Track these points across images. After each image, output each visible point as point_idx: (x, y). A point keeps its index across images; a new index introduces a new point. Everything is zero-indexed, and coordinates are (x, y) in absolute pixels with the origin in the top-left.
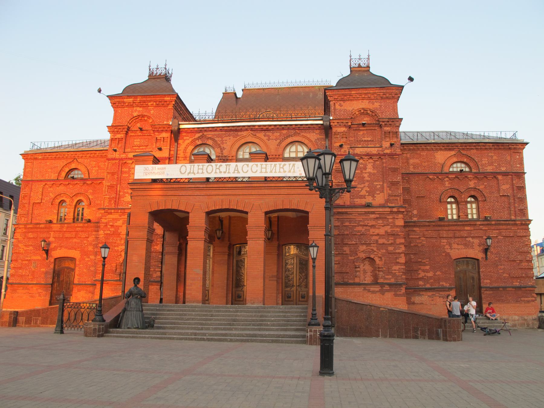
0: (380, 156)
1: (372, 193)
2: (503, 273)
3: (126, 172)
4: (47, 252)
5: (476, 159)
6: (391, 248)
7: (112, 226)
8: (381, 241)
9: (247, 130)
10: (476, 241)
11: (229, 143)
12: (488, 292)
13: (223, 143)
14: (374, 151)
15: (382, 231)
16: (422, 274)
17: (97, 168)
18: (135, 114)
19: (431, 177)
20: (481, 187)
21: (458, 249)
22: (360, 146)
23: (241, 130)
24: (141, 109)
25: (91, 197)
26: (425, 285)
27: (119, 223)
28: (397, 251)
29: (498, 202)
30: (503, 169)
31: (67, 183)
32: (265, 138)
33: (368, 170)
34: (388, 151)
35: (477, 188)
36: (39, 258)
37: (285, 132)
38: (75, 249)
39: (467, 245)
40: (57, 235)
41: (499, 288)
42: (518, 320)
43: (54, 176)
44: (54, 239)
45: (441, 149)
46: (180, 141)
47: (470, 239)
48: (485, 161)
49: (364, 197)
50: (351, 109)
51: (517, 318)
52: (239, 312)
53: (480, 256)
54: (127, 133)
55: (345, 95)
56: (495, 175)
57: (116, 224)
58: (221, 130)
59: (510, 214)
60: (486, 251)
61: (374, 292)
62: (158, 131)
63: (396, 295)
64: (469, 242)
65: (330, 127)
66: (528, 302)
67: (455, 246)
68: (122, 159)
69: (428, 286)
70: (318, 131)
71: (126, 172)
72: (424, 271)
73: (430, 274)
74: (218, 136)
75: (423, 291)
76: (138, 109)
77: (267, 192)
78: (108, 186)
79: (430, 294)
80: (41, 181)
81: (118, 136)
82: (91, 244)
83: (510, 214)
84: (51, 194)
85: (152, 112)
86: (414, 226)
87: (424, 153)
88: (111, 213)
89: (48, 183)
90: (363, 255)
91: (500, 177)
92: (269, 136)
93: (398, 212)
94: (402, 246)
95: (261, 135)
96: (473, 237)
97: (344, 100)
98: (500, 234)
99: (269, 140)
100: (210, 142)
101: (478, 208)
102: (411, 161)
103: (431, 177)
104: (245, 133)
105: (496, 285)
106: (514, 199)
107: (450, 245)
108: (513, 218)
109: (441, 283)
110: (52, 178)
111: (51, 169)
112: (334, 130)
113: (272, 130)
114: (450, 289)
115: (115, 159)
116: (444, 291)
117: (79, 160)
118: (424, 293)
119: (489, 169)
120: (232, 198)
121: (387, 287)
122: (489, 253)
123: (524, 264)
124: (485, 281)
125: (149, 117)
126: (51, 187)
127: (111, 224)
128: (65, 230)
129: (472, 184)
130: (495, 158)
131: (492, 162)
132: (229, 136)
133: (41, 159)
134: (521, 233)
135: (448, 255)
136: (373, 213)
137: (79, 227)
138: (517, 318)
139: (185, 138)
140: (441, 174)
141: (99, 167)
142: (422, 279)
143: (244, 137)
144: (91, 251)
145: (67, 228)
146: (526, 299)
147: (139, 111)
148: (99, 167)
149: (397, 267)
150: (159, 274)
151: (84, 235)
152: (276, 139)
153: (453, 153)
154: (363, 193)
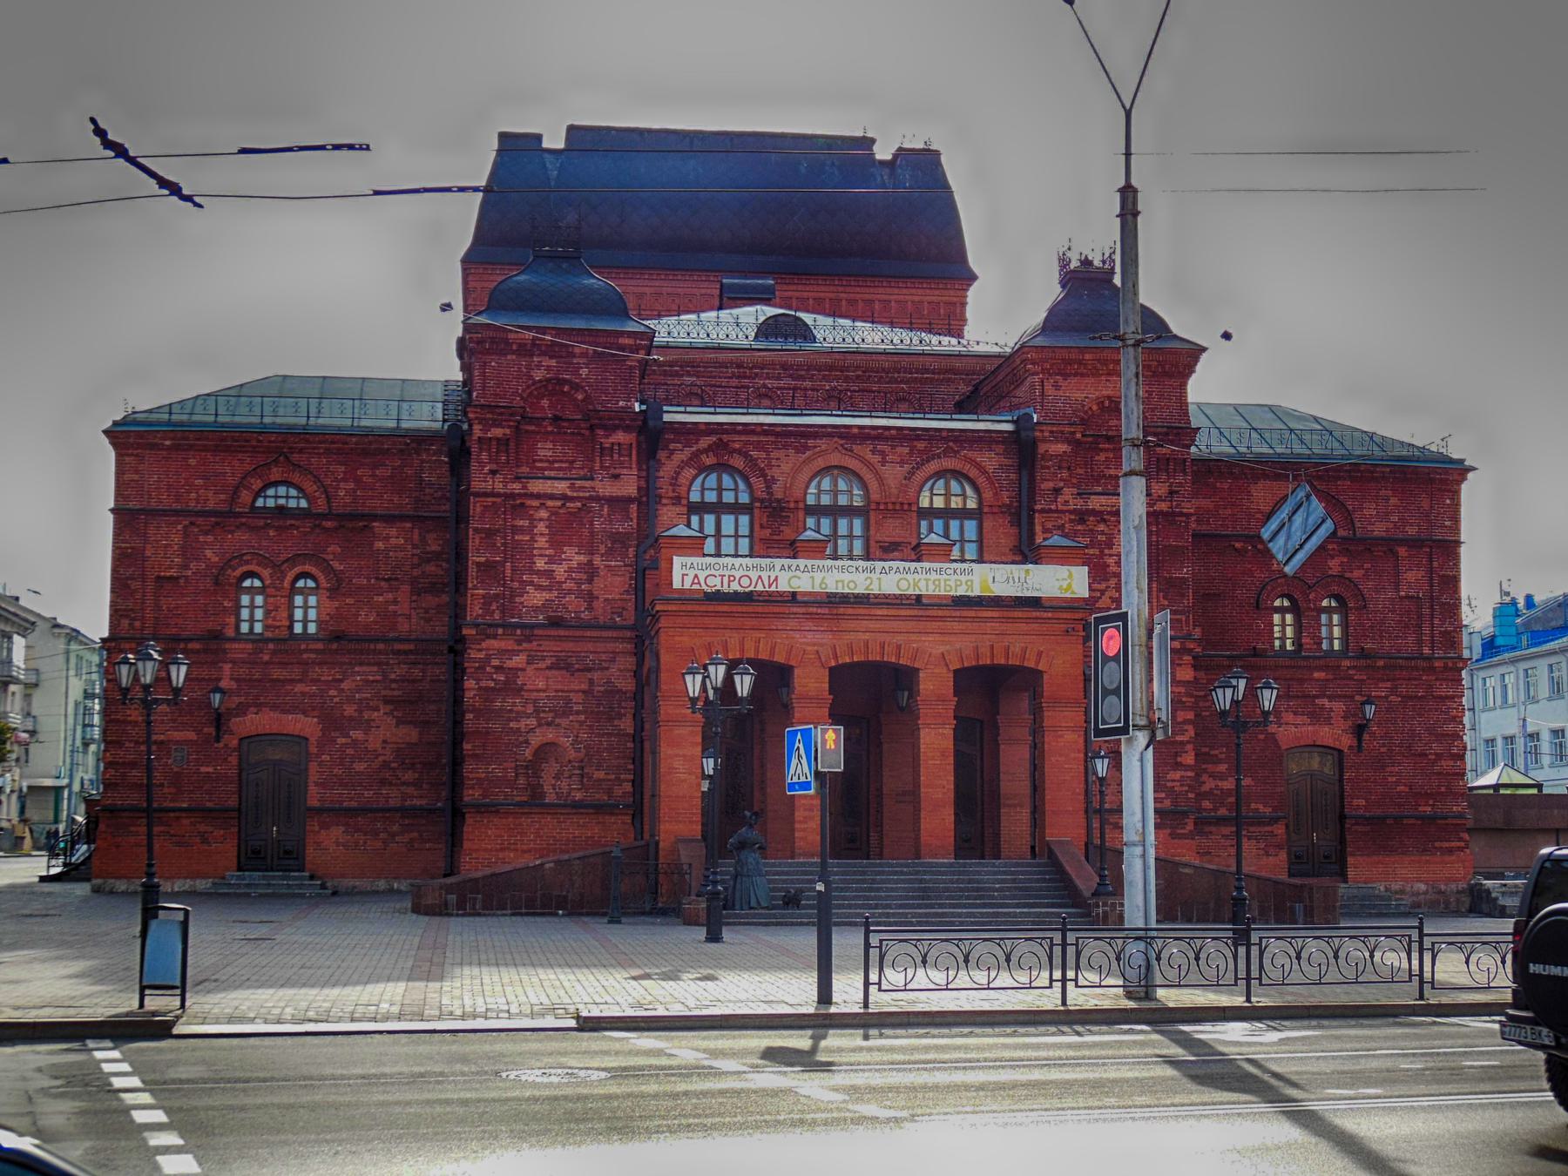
2: (1397, 783)
3: (521, 530)
4: (219, 720)
5: (1350, 505)
7: (499, 669)
9: (830, 435)
10: (1339, 707)
11: (786, 467)
12: (1359, 828)
13: (770, 466)
17: (352, 485)
18: (538, 375)
19: (1237, 545)
20: (1357, 574)
21: (1296, 726)
22: (1100, 489)
23: (815, 436)
24: (553, 363)
25: (336, 565)
26: (1215, 809)
27: (518, 660)
28: (1178, 738)
29: (1393, 611)
30: (1412, 531)
31: (261, 523)
32: (875, 459)
35: (1347, 575)
36: (192, 735)
37: (921, 445)
38: (305, 713)
39: (1318, 716)
40: (243, 671)
41: (1385, 818)
42: (1426, 893)
43: (213, 501)
44: (234, 685)
46: (662, 455)
47: (1325, 702)
48: (1370, 510)
50: (1080, 395)
51: (1423, 887)
52: (986, 872)
53: (1346, 742)
55: (1069, 362)
56: (1389, 545)
57: (509, 664)
58: (766, 433)
59: (1420, 642)
60: (1359, 730)
62: (604, 427)
64: (1322, 708)
65: (1034, 443)
66: (1450, 851)
68: (512, 496)
70: (1000, 448)
71: (521, 530)
72: (1213, 776)
74: (759, 446)
75: (1210, 824)
76: (547, 362)
77: (956, 626)
78: (478, 564)
80: (176, 513)
82: (350, 700)
83: (1420, 642)
84: (209, 553)
85: (584, 372)
88: (495, 637)
89: (200, 521)
91: (1402, 551)
92: (883, 453)
94: (1190, 727)
95: (865, 450)
96: (1331, 698)
97: (1065, 376)
98: (1393, 691)
99: (884, 462)
100: (738, 462)
101: (1345, 625)
103: (1237, 545)
104: (823, 444)
106: (1432, 607)
108: (1426, 651)
109: (1253, 806)
110: (211, 505)
111: (205, 478)
112: (1042, 448)
113: (893, 438)
114: (1273, 820)
115: (493, 494)
116: (1260, 824)
117: (295, 457)
118: (1213, 829)
119: (1379, 530)
120: (887, 638)
122: (1366, 736)
123: (1446, 764)
124: (1355, 802)
125: (576, 387)
126: (206, 533)
127: (496, 662)
128: (266, 658)
130: (1393, 501)
131: (1387, 514)
132: (785, 447)
133: (169, 448)
134: (1444, 690)
137: (312, 651)
138: (1423, 887)
139: (672, 446)
141: (358, 481)
143: (822, 453)
144: (351, 719)
145: (274, 653)
146: (1446, 845)
147: (548, 368)
148: (358, 481)
149: (1178, 775)
150: (628, 787)
151: (326, 674)
152: (902, 463)
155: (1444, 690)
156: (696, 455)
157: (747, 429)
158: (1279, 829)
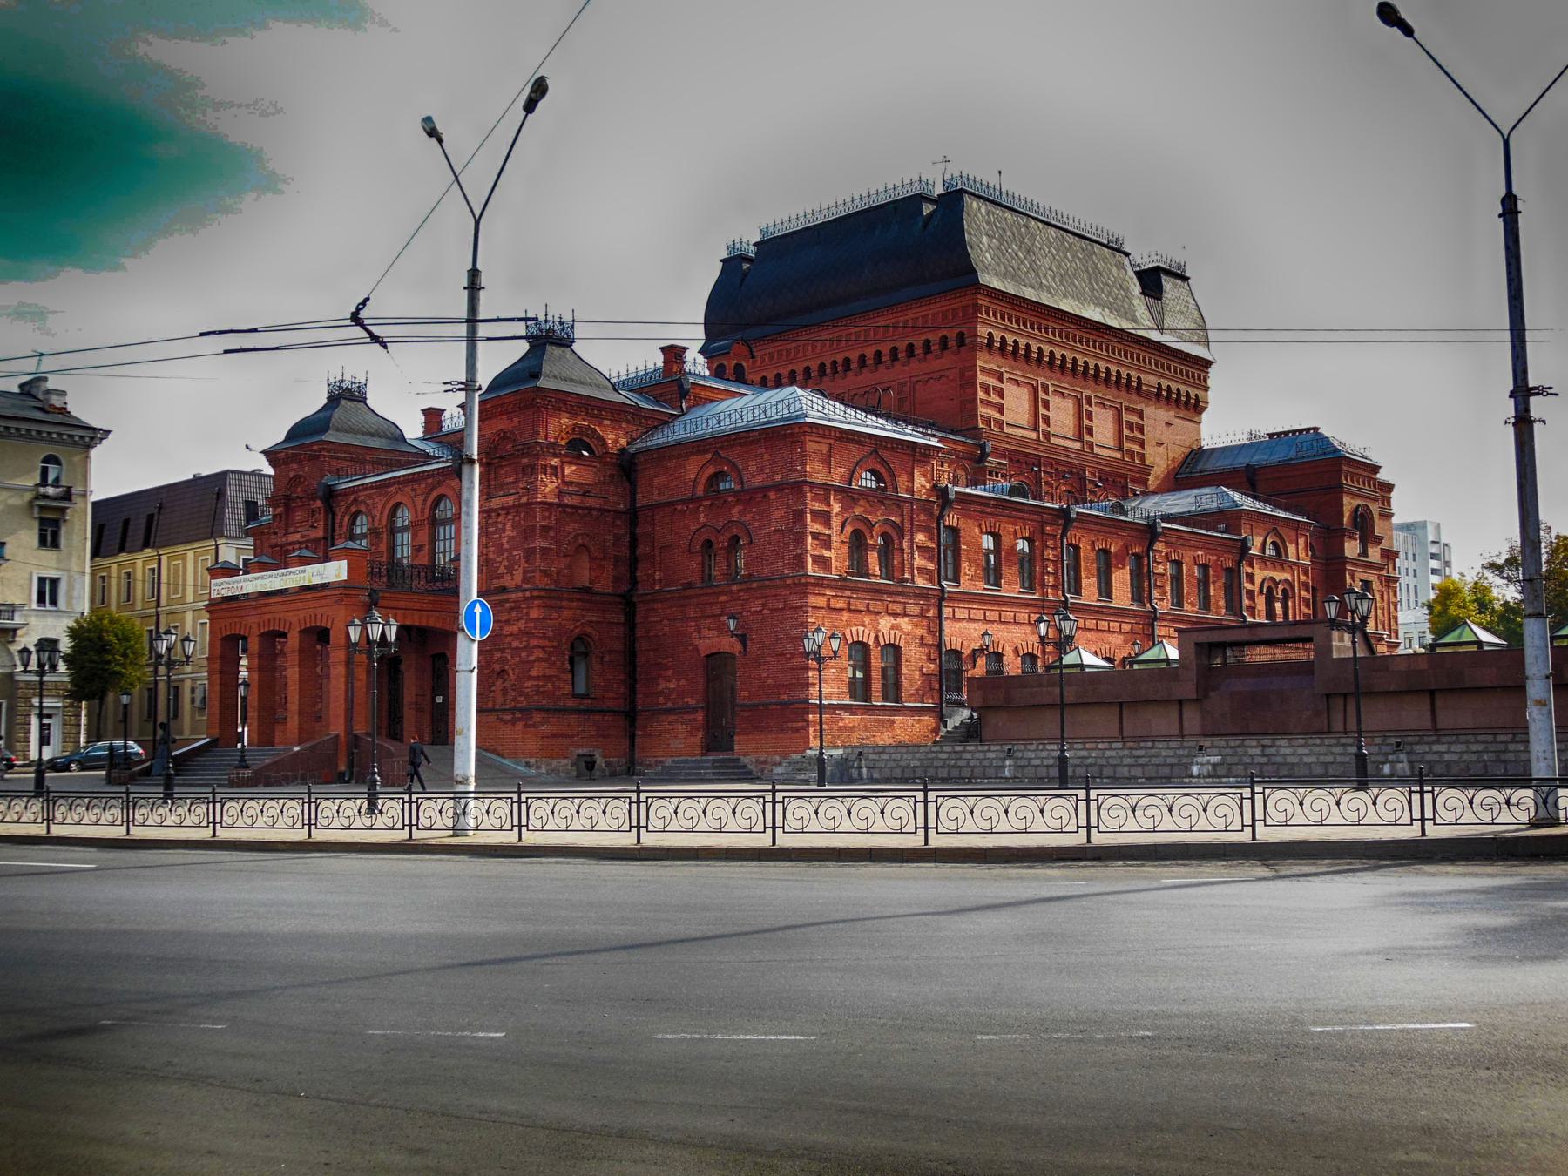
0: (517, 508)
1: (510, 569)
6: (524, 654)
8: (515, 644)
14: (510, 500)
15: (514, 629)
30: (778, 478)
33: (508, 532)
34: (524, 499)
45: (693, 454)
49: (501, 576)
54: (287, 507)
56: (764, 490)
61: (506, 722)
63: (526, 726)
66: (797, 730)
67: (705, 632)
68: (282, 546)
69: (670, 705)
73: (672, 685)
77: (300, 605)
79: (671, 718)
81: (279, 510)
86: (654, 601)
90: (497, 667)
91: (772, 495)
93: (532, 598)
98: (764, 605)
102: (657, 482)
104: (392, 489)
105: (755, 701)
114: (694, 710)
119: (758, 481)
121: (518, 715)
134: (795, 602)
136: (507, 601)
140: (691, 500)
142: (661, 693)
149: (528, 684)
153: (709, 456)
154: (502, 570)
155: (795, 602)
156: (348, 508)
157: (365, 487)
158: (700, 716)
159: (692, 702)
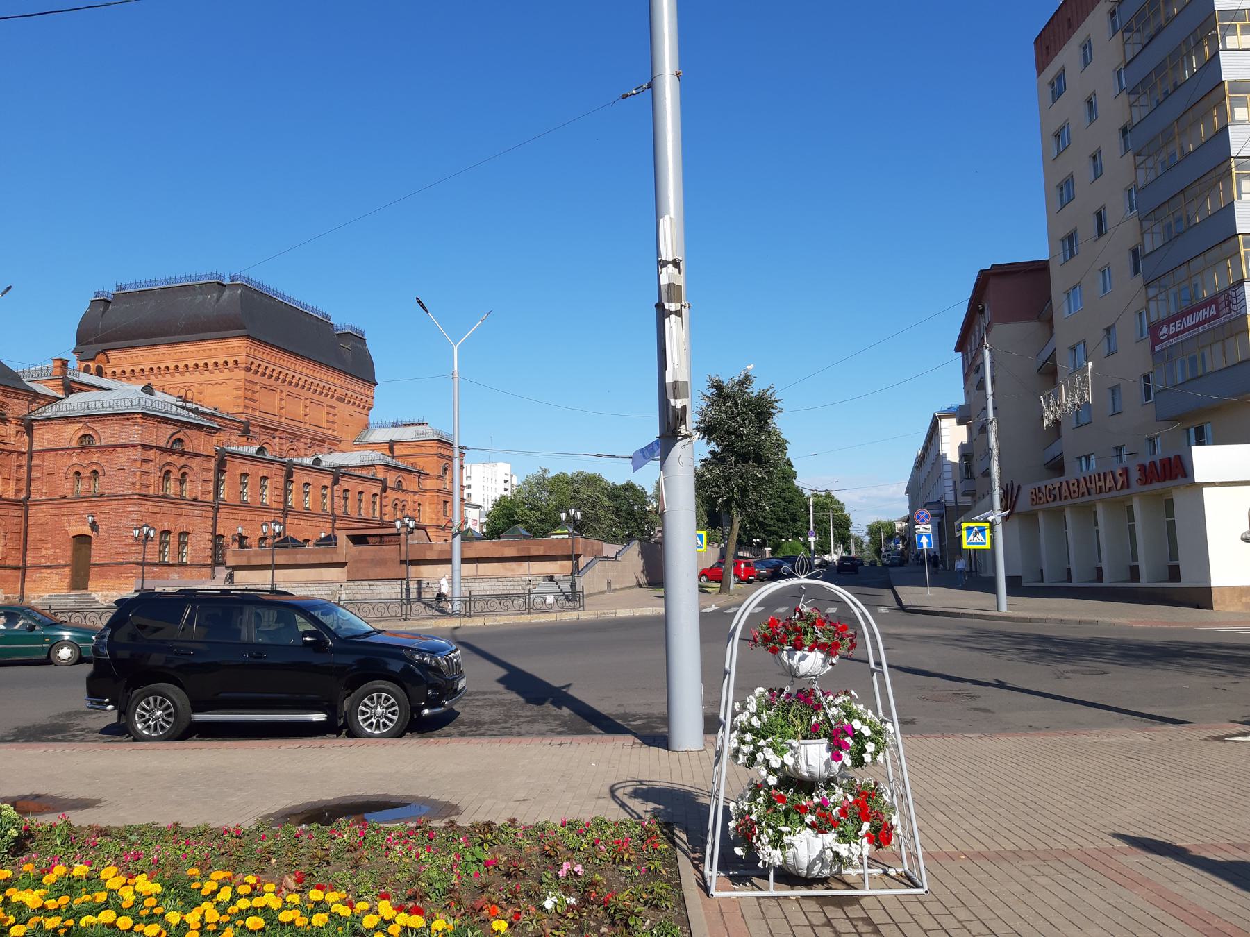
5: (100, 432)
16: (44, 552)
20: (103, 461)
30: (122, 441)
39: (83, 522)
56: (114, 447)
73: (50, 552)
79: (49, 571)
87: (57, 427)
107: (69, 522)
114: (64, 566)
119: (110, 442)
129: (95, 458)
135: (67, 532)
158: (67, 570)
159: (63, 562)
